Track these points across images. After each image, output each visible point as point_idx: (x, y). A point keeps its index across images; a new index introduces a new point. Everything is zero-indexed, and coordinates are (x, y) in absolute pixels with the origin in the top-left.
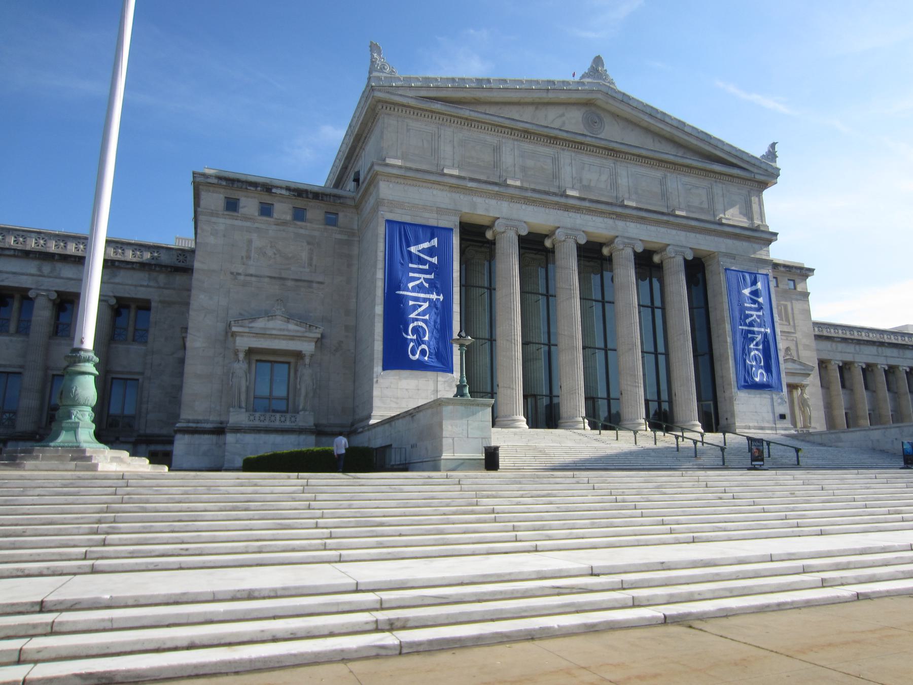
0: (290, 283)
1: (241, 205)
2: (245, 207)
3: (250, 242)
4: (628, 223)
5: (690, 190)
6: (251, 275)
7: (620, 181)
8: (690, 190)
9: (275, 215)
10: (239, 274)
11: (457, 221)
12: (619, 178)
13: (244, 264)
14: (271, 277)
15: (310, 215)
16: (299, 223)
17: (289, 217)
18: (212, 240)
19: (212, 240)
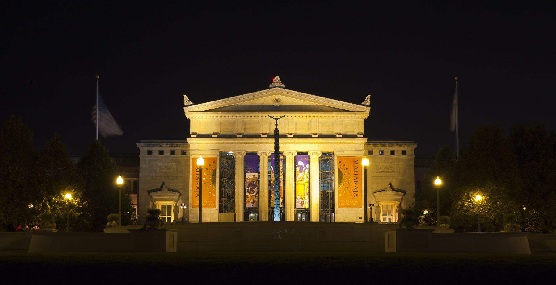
0: (170, 178)
1: (153, 152)
2: (154, 153)
3: (157, 164)
4: (290, 145)
5: (324, 124)
6: (158, 176)
7: (287, 127)
8: (324, 124)
9: (164, 154)
10: (153, 176)
11: (217, 153)
12: (287, 125)
13: (155, 172)
14: (164, 176)
15: (176, 152)
16: (172, 156)
17: (169, 154)
18: (144, 166)
19: (144, 166)
